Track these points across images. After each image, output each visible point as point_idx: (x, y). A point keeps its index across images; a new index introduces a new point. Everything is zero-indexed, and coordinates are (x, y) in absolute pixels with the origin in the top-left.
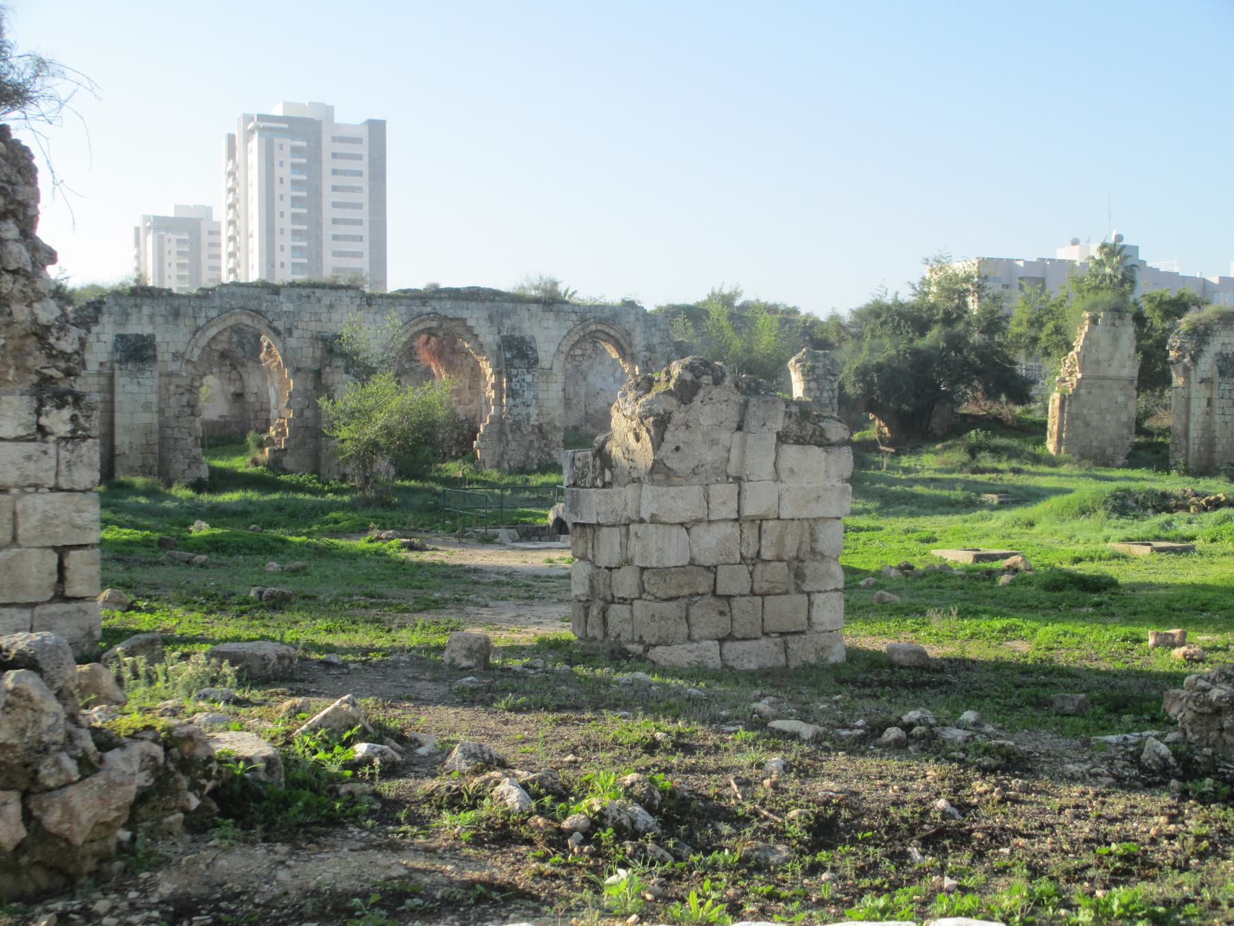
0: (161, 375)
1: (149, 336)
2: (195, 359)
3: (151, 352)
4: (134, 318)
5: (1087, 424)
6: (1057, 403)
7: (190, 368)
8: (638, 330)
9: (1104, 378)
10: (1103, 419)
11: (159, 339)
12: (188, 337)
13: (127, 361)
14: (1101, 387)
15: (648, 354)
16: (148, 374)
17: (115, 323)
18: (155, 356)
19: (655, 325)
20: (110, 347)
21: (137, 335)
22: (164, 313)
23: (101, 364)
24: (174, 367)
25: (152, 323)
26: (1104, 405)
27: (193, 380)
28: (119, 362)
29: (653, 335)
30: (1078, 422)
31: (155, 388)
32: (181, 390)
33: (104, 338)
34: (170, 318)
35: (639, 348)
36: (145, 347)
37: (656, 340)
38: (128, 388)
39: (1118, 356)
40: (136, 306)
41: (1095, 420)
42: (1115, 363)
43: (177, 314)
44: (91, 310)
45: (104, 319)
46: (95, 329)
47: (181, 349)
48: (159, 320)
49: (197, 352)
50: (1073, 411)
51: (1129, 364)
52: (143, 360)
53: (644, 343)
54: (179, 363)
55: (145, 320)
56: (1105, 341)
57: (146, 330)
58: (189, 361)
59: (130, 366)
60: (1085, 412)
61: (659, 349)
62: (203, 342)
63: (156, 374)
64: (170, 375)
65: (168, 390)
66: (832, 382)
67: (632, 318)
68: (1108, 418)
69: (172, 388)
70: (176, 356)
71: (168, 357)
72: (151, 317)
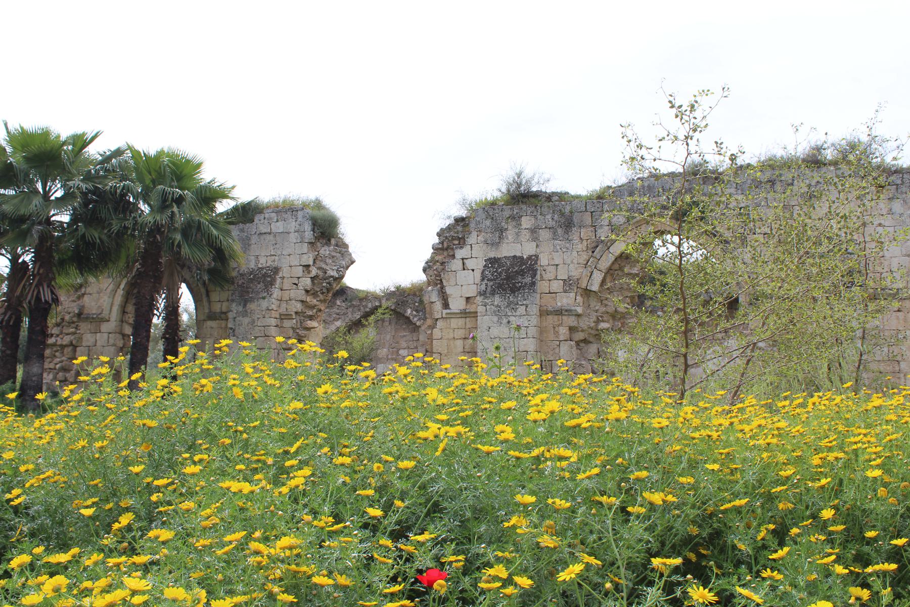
0: (544, 313)
1: (530, 258)
2: (595, 287)
3: (528, 280)
4: (510, 235)
7: (594, 304)
11: (544, 261)
12: (585, 256)
13: (493, 293)
16: (521, 310)
17: (486, 242)
18: (533, 284)
20: (478, 275)
21: (515, 257)
22: (551, 223)
23: (468, 299)
24: (566, 300)
25: (535, 239)
27: (598, 321)
28: (482, 294)
31: (532, 331)
32: (580, 336)
33: (470, 264)
34: (560, 231)
36: (522, 273)
38: (495, 331)
40: (512, 218)
43: (568, 224)
44: (459, 228)
45: (472, 239)
46: (460, 253)
47: (576, 272)
48: (545, 235)
49: (598, 277)
52: (514, 290)
54: (572, 295)
55: (525, 235)
57: (527, 249)
58: (587, 293)
59: (497, 300)
62: (606, 261)
63: (534, 310)
64: (559, 312)
65: (556, 333)
69: (563, 331)
70: (569, 284)
71: (557, 286)
72: (534, 231)
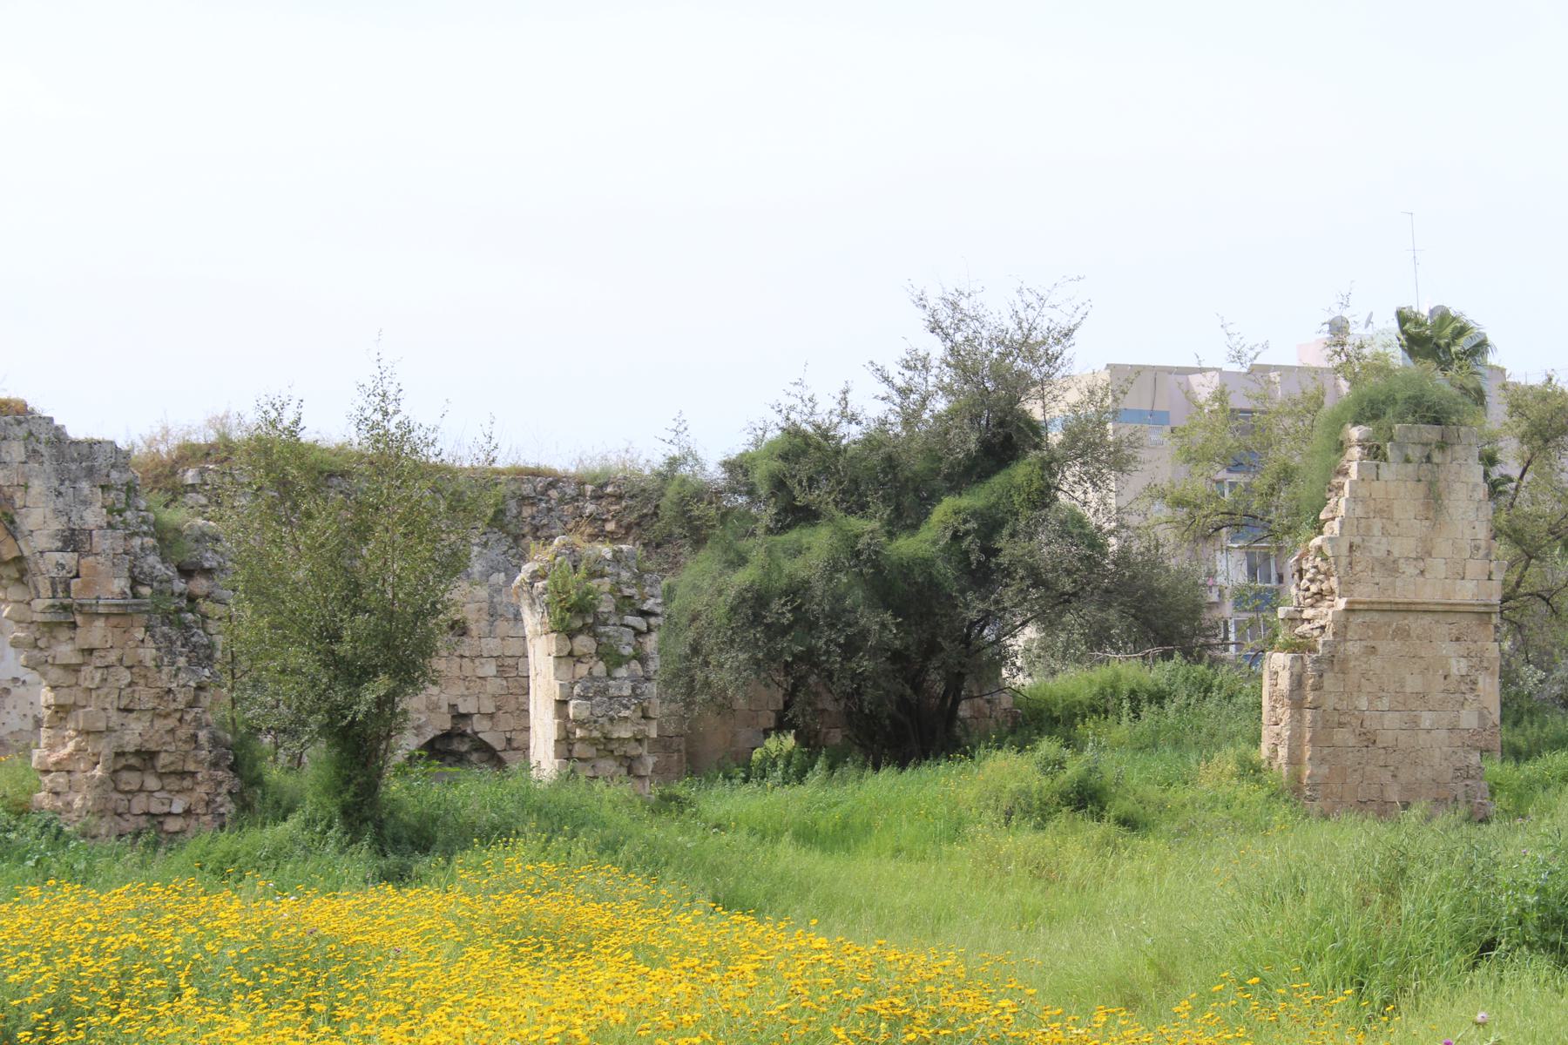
5: (1369, 740)
6: (1284, 682)
8: (37, 486)
9: (1408, 609)
10: (1413, 725)
14: (1403, 634)
15: (69, 558)
19: (90, 472)
26: (1413, 683)
29: (86, 503)
30: (1342, 736)
35: (42, 541)
37: (93, 517)
39: (1443, 547)
41: (1390, 725)
42: (1438, 567)
50: (1330, 702)
51: (1475, 567)
53: (56, 525)
56: (1407, 507)
60: (1363, 703)
61: (104, 542)
66: (638, 633)
67: (16, 451)
68: (1426, 719)
